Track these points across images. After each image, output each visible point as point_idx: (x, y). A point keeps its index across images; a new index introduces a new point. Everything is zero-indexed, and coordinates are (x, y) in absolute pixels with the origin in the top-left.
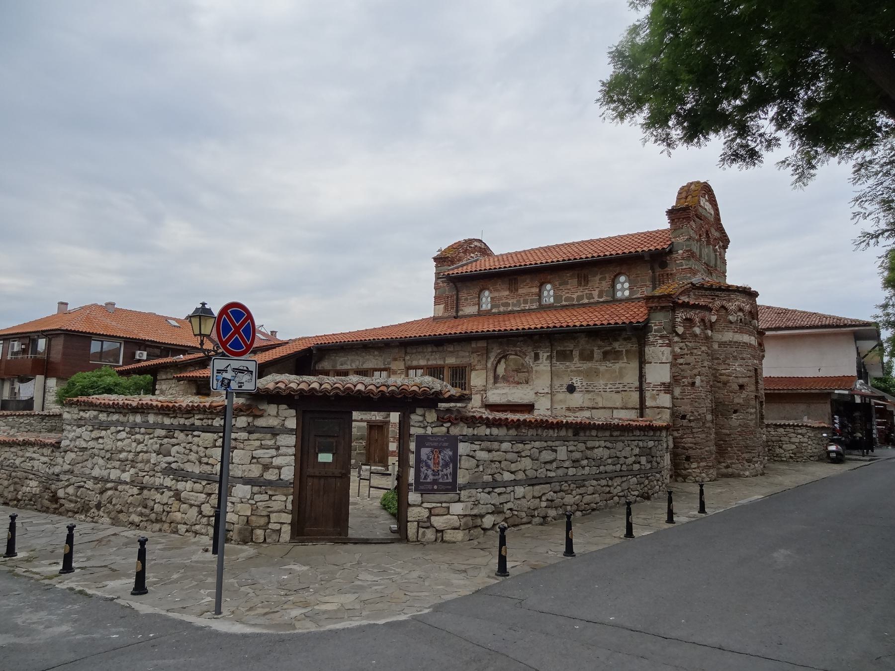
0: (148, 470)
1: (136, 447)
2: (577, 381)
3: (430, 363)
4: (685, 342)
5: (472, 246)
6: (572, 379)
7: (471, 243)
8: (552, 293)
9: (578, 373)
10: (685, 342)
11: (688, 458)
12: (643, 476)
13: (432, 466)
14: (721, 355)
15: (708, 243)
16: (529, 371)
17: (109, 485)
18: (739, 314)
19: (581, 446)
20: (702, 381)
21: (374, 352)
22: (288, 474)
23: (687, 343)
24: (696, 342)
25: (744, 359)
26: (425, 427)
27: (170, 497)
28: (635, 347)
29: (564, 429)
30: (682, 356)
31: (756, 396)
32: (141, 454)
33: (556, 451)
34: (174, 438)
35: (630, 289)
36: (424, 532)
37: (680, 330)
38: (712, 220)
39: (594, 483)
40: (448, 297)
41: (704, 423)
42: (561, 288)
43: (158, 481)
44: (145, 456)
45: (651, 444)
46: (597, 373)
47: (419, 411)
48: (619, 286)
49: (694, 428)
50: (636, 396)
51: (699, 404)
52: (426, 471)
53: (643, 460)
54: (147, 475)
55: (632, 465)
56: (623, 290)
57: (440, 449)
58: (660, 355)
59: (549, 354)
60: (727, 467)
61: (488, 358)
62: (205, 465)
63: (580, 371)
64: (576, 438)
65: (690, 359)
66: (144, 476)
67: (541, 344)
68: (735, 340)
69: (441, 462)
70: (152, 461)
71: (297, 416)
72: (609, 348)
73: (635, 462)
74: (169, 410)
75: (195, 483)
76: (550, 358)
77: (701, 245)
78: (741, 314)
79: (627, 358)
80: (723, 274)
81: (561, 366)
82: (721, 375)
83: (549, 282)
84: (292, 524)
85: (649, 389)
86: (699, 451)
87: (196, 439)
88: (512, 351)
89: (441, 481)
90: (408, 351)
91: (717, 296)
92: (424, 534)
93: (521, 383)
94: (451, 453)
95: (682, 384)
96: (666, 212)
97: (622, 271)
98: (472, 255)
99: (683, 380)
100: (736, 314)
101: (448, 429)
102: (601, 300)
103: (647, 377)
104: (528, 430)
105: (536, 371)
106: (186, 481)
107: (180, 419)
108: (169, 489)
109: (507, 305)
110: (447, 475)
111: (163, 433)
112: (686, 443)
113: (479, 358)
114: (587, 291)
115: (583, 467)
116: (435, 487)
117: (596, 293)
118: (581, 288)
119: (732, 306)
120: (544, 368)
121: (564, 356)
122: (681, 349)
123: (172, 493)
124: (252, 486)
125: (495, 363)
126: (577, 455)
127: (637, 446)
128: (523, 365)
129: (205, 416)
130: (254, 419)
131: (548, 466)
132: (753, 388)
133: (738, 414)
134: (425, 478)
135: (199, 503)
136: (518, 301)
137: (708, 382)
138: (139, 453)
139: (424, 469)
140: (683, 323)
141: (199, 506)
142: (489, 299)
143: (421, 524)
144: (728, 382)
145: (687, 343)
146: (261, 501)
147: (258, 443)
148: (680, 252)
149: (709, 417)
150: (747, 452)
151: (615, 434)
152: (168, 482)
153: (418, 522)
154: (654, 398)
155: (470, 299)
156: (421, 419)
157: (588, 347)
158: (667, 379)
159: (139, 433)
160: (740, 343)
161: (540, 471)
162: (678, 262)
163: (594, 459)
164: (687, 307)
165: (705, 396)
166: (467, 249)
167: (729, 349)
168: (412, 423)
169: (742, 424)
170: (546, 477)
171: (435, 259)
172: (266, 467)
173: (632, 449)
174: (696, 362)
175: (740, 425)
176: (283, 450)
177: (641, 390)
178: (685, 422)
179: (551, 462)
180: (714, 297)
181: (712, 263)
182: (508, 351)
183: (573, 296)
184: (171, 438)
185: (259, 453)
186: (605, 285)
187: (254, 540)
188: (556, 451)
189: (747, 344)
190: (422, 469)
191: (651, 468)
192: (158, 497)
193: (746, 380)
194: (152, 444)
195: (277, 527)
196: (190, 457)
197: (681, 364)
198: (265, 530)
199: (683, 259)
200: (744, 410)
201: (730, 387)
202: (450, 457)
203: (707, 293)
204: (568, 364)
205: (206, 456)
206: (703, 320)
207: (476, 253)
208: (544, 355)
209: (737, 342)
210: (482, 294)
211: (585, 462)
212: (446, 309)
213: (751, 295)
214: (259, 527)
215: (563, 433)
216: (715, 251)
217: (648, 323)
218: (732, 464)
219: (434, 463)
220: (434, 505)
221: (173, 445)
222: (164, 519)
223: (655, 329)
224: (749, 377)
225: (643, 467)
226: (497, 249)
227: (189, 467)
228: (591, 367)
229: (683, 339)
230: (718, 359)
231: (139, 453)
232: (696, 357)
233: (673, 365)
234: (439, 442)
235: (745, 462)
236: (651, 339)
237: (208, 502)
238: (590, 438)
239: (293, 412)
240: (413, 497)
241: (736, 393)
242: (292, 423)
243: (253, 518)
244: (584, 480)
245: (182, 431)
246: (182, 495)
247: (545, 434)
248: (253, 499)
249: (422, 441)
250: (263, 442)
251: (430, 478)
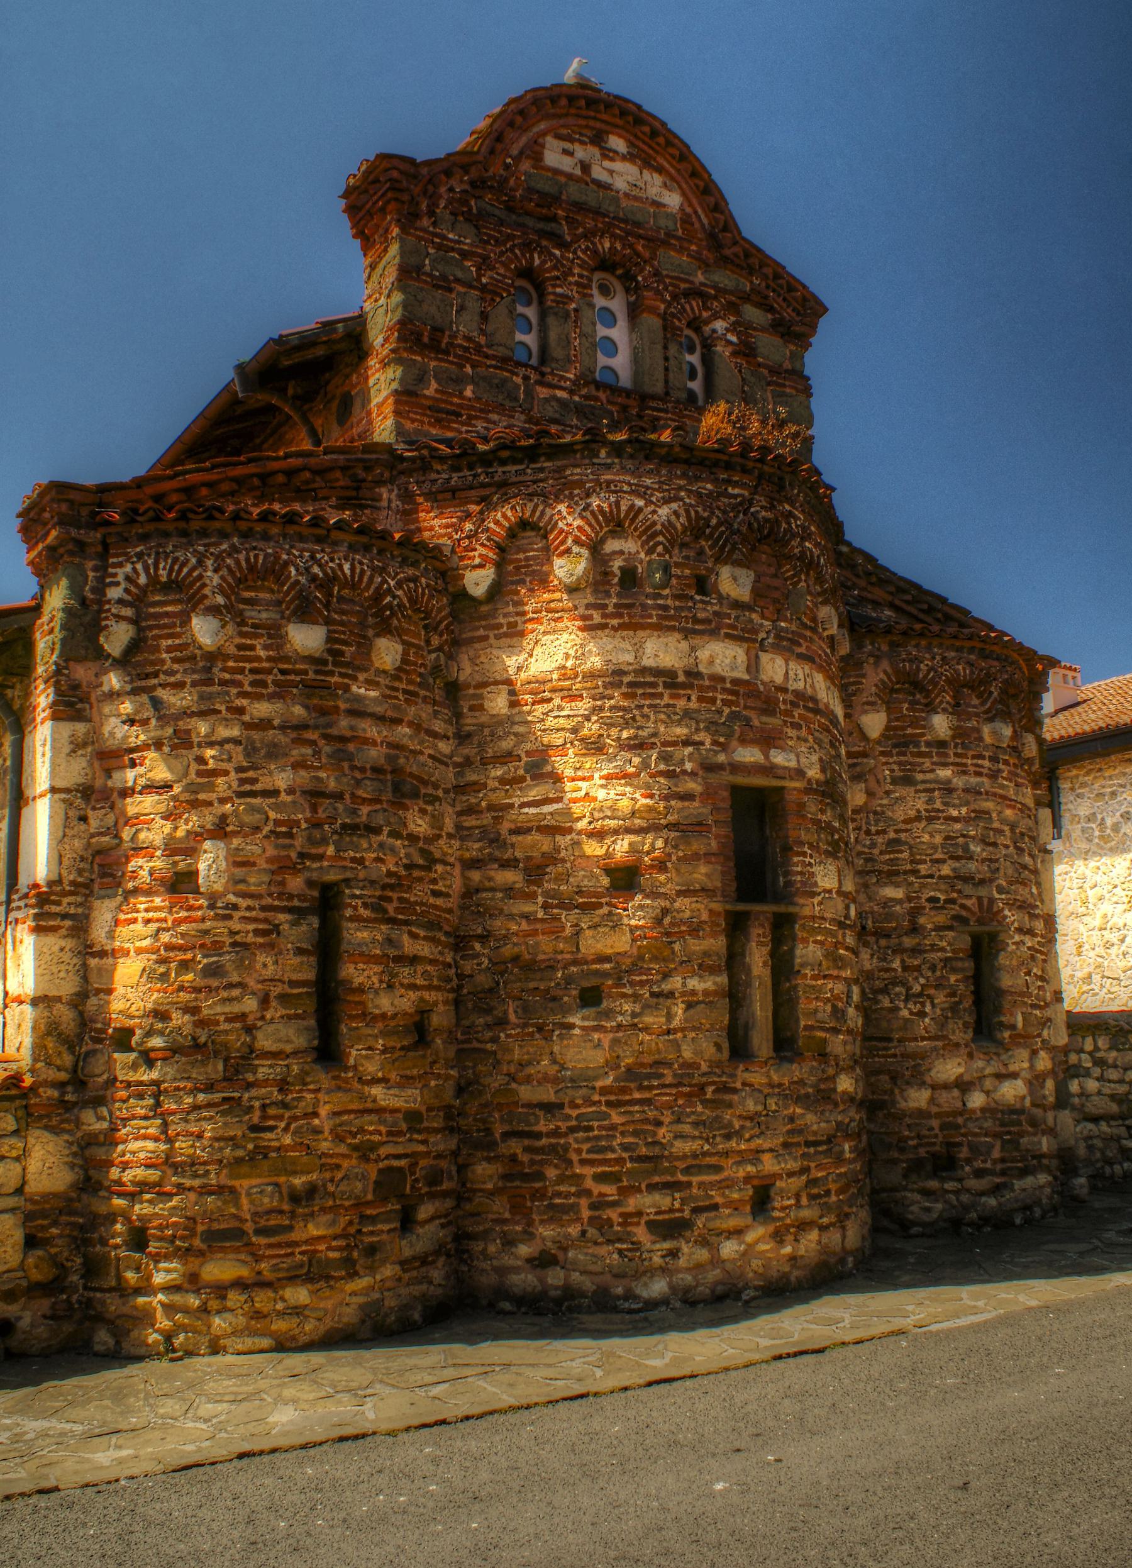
10: (154, 688)
18: (612, 545)
23: (162, 693)
144: (552, 858)
145: (162, 693)
150: (652, 1188)
180: (487, 492)
189: (670, 673)
200: (642, 983)
235: (641, 1233)
241: (600, 905)
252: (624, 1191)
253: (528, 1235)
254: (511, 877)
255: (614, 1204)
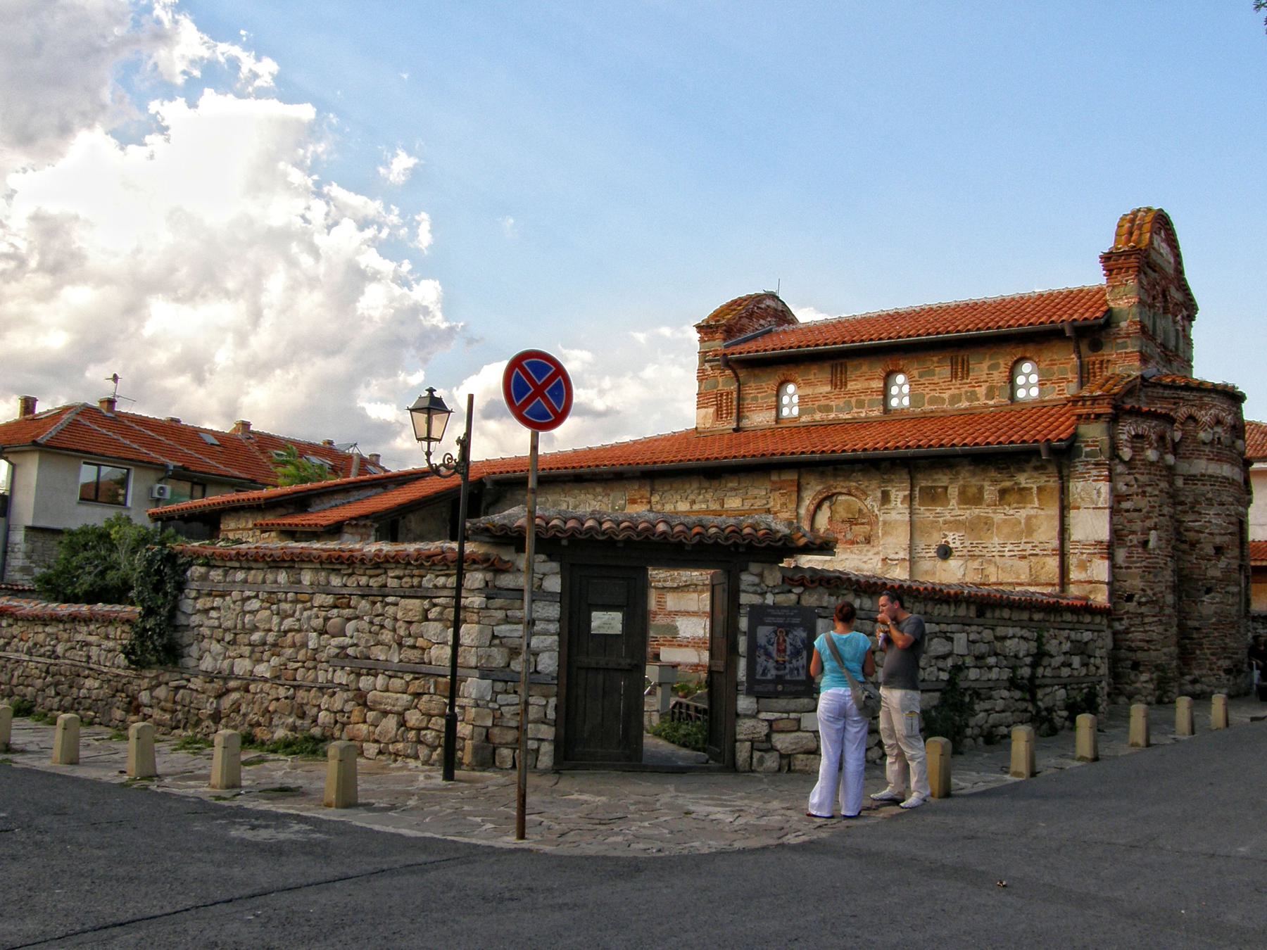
0: (304, 659)
1: (281, 624)
2: (954, 540)
3: (696, 507)
4: (1133, 474)
5: (763, 306)
6: (946, 536)
7: (760, 301)
8: (906, 389)
9: (956, 525)
11: (1136, 666)
12: (1076, 686)
13: (774, 654)
14: (1187, 497)
15: (1166, 311)
16: (873, 523)
17: (232, 684)
19: (988, 635)
20: (1160, 539)
21: (594, 489)
22: (548, 663)
23: (1137, 476)
24: (1150, 474)
25: (1224, 505)
26: (763, 594)
27: (347, 701)
28: (1053, 483)
29: (964, 606)
30: (1127, 497)
31: (1240, 566)
32: (290, 635)
33: (951, 640)
34: (350, 607)
35: (1041, 384)
36: (762, 757)
37: (1126, 453)
38: (1172, 272)
39: (1005, 693)
40: (722, 395)
41: (1162, 608)
42: (922, 381)
43: (322, 677)
44: (298, 637)
45: (1087, 636)
46: (988, 523)
47: (754, 567)
48: (1020, 380)
49: (1147, 616)
50: (1053, 563)
51: (1156, 576)
52: (765, 663)
53: (1076, 661)
54: (303, 667)
55: (1059, 668)
56: (1027, 386)
57: (788, 628)
58: (1095, 497)
59: (907, 493)
60: (1194, 682)
61: (799, 500)
62: (409, 650)
63: (962, 523)
64: (981, 621)
65: (1142, 503)
66: (296, 670)
67: (893, 477)
68: (1210, 471)
69: (789, 648)
70: (311, 645)
71: (562, 573)
72: (1007, 484)
73: (1064, 664)
74: (342, 563)
75: (390, 677)
76: (911, 498)
77: (1155, 314)
78: (1219, 429)
79: (1039, 499)
80: (1187, 363)
81: (928, 514)
82: (1187, 530)
83: (901, 371)
84: (556, 742)
85: (1076, 551)
86: (1153, 653)
87: (390, 610)
88: (842, 487)
89: (788, 677)
90: (656, 487)
91: (1182, 398)
92: (761, 761)
93: (858, 543)
94: (804, 635)
95: (1129, 544)
96: (1101, 257)
97: (1028, 355)
98: (762, 322)
99: (1130, 537)
100: (1212, 429)
101: (799, 598)
102: (991, 403)
103: (1072, 531)
104: (913, 603)
105: (885, 523)
106: (376, 676)
107: (359, 578)
108: (345, 688)
109: (828, 409)
110: (797, 669)
111: (330, 600)
112: (1132, 641)
113: (783, 500)
114: (966, 388)
115: (990, 668)
116: (780, 688)
117: (982, 391)
118: (957, 383)
119: (1205, 416)
120: (899, 517)
121: (934, 496)
122: (1127, 485)
123: (351, 694)
124: (494, 680)
125: (812, 507)
126: (983, 648)
127: (1068, 638)
128: (860, 511)
129: (407, 572)
130: (495, 575)
131: (941, 664)
132: (1236, 552)
133: (1212, 594)
134: (764, 673)
135: (400, 709)
136: (848, 404)
137: (1168, 541)
138: (286, 632)
139: (761, 660)
140: (1132, 442)
141: (401, 714)
142: (796, 399)
143: (756, 745)
144: (1198, 542)
145: (1137, 476)
146: (508, 705)
147: (500, 614)
148: (1123, 324)
149: (1170, 599)
150: (1225, 658)
151: (1037, 617)
152: (341, 677)
153: (752, 741)
154: (1083, 566)
155: (763, 398)
156: (756, 580)
157: (974, 481)
158: (1104, 534)
159: (286, 601)
160: (1217, 477)
161: (929, 670)
162: (1119, 341)
163: (1005, 657)
164: (1137, 416)
165: (1165, 564)
166: (753, 312)
167: (1200, 488)
168: (743, 587)
169: (1219, 611)
170: (937, 680)
171: (700, 328)
172: (514, 652)
173: (1061, 643)
174: (1151, 507)
175: (1216, 613)
176: (539, 626)
177: (1063, 554)
178: (1131, 606)
179: (944, 657)
181: (1172, 344)
182: (836, 488)
183: (943, 395)
184: (344, 608)
185: (503, 629)
186: (999, 376)
187: (497, 764)
188: (951, 640)
189: (1228, 479)
190: (758, 660)
191: (1087, 675)
192: (324, 701)
193: (1227, 538)
194: (309, 618)
195: (532, 745)
196: (380, 638)
197: (1128, 511)
198: (514, 750)
199: (1128, 335)
201: (1201, 549)
202: (803, 641)
203: (1167, 393)
204: (939, 509)
205: (410, 635)
206: (1162, 438)
207: (769, 319)
208: (898, 494)
209: (1211, 476)
210: (783, 389)
211: (992, 660)
212: (718, 415)
213: (1234, 397)
214: (506, 745)
215: (962, 611)
216: (1175, 322)
217: (1074, 442)
218: (1201, 677)
219: (778, 650)
220: (777, 715)
221: (349, 620)
222: (337, 734)
223: (1086, 452)
224: (1230, 534)
225: (1076, 673)
226: (805, 315)
227: (379, 653)
228: (979, 517)
229: (1131, 468)
230: (1182, 503)
231: (286, 632)
232: (1151, 499)
233: (1114, 511)
234: (785, 616)
235: (1222, 673)
236: (1080, 468)
237: (416, 707)
238: (1001, 622)
239: (555, 566)
240: (744, 703)
242: (554, 584)
243: (496, 731)
244: (991, 689)
245: (363, 596)
246: (370, 696)
247: (936, 612)
248: (496, 701)
249: (758, 614)
250: (509, 613)
251: (772, 674)
252: (1218, 659)
253: (1190, 674)
254: (1185, 547)
255: (1215, 663)
